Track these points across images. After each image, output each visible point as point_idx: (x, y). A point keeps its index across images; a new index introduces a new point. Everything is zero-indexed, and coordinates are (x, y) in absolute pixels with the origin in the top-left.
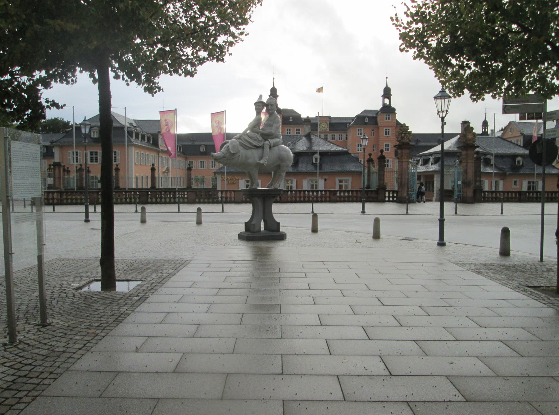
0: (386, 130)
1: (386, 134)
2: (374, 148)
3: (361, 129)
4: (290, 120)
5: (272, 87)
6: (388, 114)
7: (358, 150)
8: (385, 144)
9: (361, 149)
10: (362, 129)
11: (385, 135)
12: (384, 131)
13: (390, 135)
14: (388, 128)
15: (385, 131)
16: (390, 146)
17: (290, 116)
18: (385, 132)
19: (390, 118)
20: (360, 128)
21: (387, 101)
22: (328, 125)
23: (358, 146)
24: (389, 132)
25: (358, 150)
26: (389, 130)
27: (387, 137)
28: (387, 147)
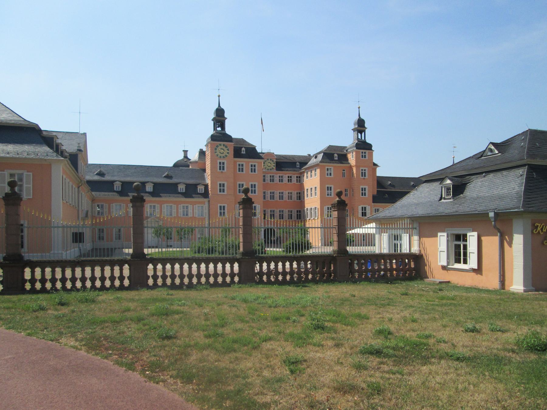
0: (362, 170)
1: (362, 176)
4: (242, 153)
5: (217, 106)
6: (364, 151)
7: (328, 195)
9: (331, 193)
11: (361, 177)
13: (367, 177)
15: (361, 171)
17: (242, 147)
23: (328, 190)
24: (365, 173)
26: (365, 170)
27: (364, 179)
28: (364, 192)
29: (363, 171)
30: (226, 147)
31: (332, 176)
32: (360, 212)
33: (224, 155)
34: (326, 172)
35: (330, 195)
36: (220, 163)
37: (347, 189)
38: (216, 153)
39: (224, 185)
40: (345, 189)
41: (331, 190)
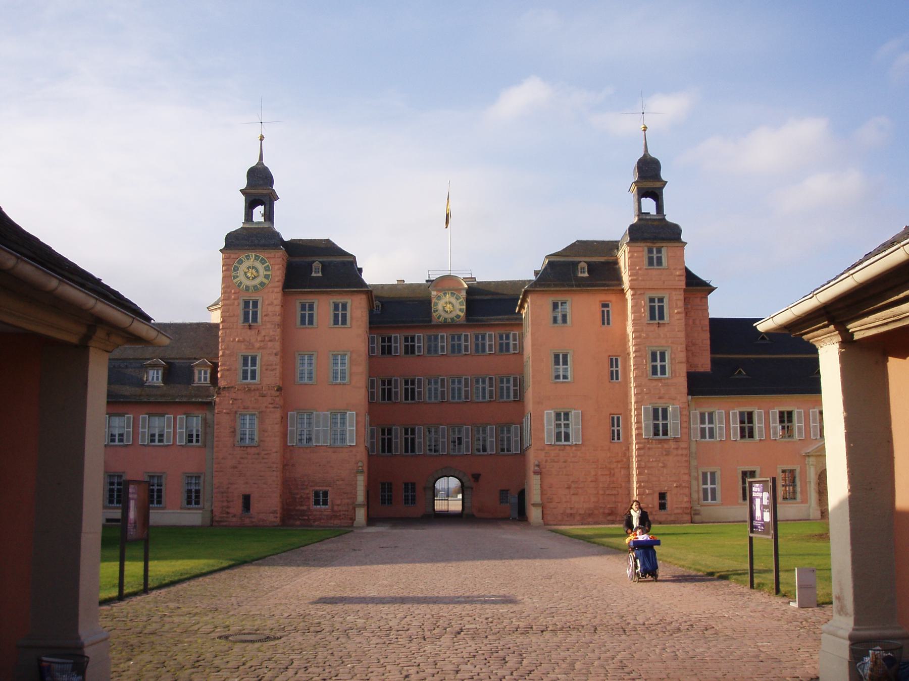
1: (652, 317)
4: (313, 274)
9: (566, 370)
15: (648, 304)
17: (314, 262)
19: (664, 260)
21: (649, 205)
22: (461, 304)
23: (557, 362)
24: (661, 309)
25: (557, 377)
29: (657, 304)
30: (263, 262)
33: (257, 282)
35: (565, 377)
36: (246, 303)
38: (235, 281)
39: (254, 360)
40: (612, 360)
41: (565, 362)
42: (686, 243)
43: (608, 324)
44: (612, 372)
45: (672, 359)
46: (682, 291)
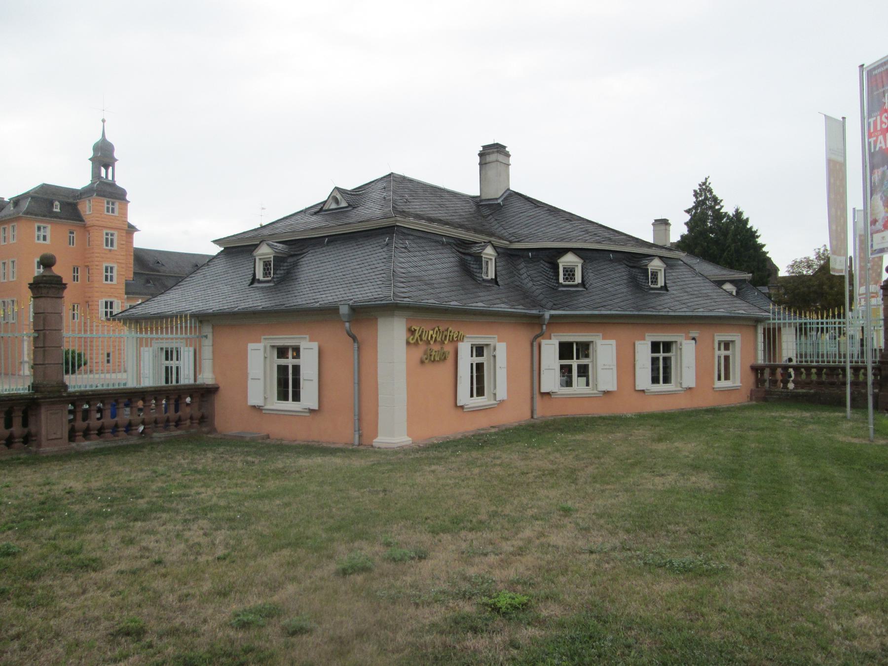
0: (107, 234)
1: (107, 245)
2: (76, 274)
3: (44, 228)
8: (105, 265)
10: (49, 227)
11: (105, 247)
12: (103, 237)
13: (115, 247)
14: (112, 232)
15: (105, 237)
16: (115, 271)
18: (105, 239)
20: (42, 225)
24: (112, 241)
26: (112, 235)
27: (110, 250)
28: (109, 274)
29: (109, 237)
31: (48, 242)
32: (102, 310)
34: (37, 233)
37: (77, 269)
40: (74, 268)
42: (129, 202)
43: (73, 245)
44: (74, 276)
45: (118, 271)
46: (125, 232)
